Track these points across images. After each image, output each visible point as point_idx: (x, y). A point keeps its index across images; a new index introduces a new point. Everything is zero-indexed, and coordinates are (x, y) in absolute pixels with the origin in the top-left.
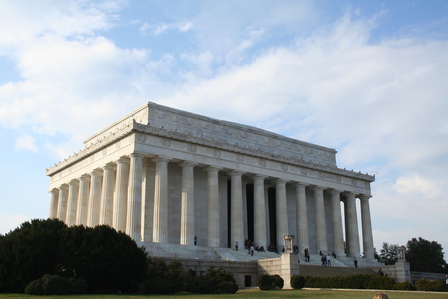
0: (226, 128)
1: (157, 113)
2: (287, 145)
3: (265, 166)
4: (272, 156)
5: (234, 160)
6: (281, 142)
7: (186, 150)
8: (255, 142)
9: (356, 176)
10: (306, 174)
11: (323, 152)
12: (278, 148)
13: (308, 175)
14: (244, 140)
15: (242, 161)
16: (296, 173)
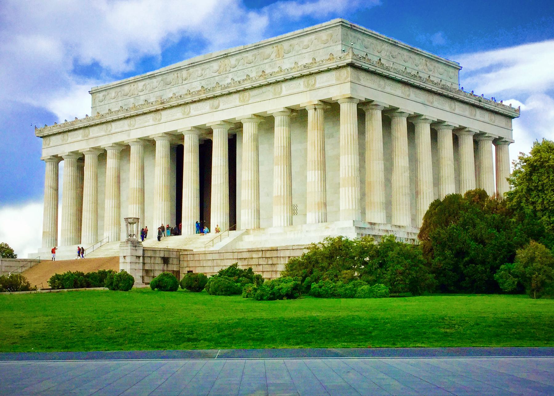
0: (165, 76)
1: (99, 97)
2: (247, 57)
3: (160, 120)
4: (162, 103)
5: (127, 128)
6: (238, 57)
7: (80, 138)
8: (201, 78)
9: (306, 72)
10: (219, 106)
11: (313, 37)
12: (232, 70)
13: (221, 107)
14: (186, 82)
15: (134, 126)
16: (204, 111)
